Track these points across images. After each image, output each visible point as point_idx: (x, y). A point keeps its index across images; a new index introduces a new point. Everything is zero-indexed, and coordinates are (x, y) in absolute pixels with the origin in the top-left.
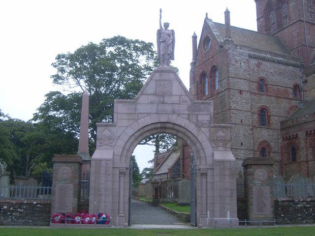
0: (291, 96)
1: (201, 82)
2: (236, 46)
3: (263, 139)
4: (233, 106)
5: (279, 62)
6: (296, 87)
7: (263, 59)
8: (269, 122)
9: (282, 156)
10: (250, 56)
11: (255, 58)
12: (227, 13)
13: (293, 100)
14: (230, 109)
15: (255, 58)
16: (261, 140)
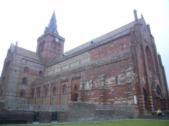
0: (38, 75)
1: (6, 66)
2: (18, 54)
3: (23, 89)
4: (11, 75)
5: (35, 62)
6: (41, 72)
7: (29, 60)
8: (27, 83)
9: (30, 96)
10: (23, 59)
11: (25, 59)
12: (17, 43)
13: (38, 76)
14: (9, 77)
15: (25, 59)
16: (21, 89)
